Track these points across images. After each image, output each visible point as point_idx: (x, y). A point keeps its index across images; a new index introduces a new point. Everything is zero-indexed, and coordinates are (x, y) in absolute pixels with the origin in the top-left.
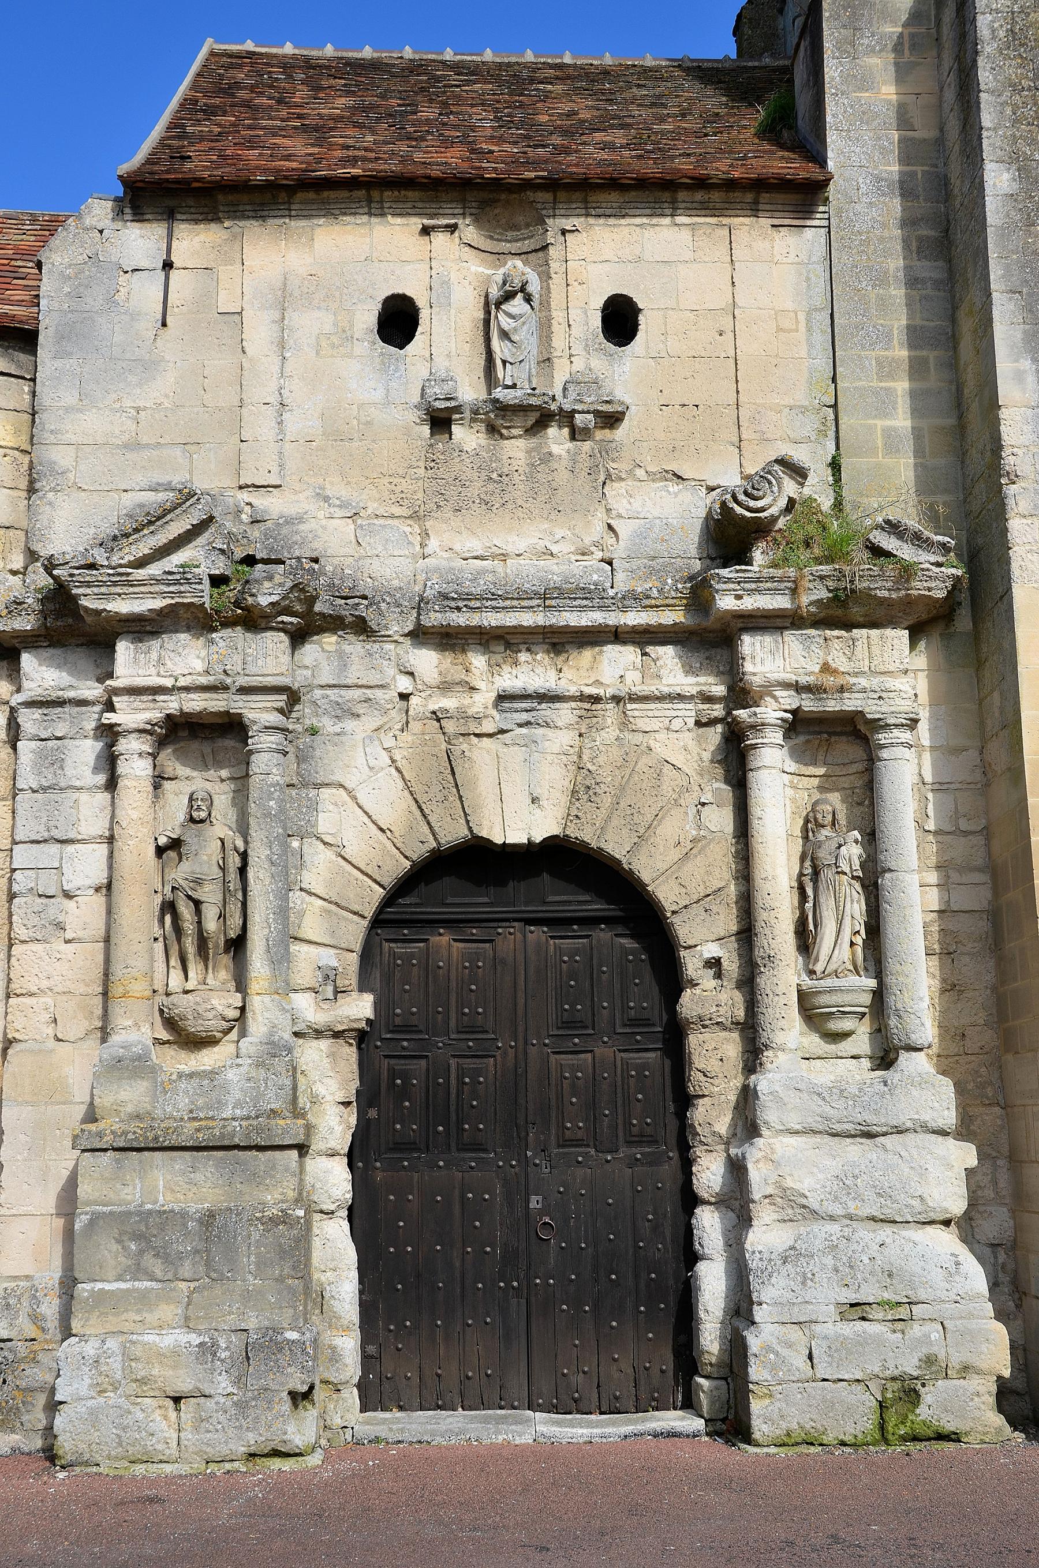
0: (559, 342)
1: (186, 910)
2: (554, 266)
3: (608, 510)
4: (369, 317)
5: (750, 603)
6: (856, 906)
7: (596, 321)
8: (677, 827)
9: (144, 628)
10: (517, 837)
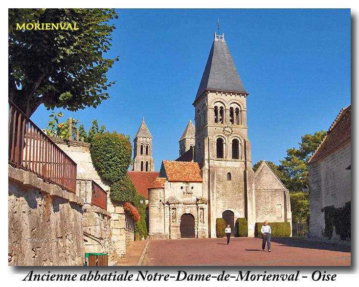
9: (171, 204)
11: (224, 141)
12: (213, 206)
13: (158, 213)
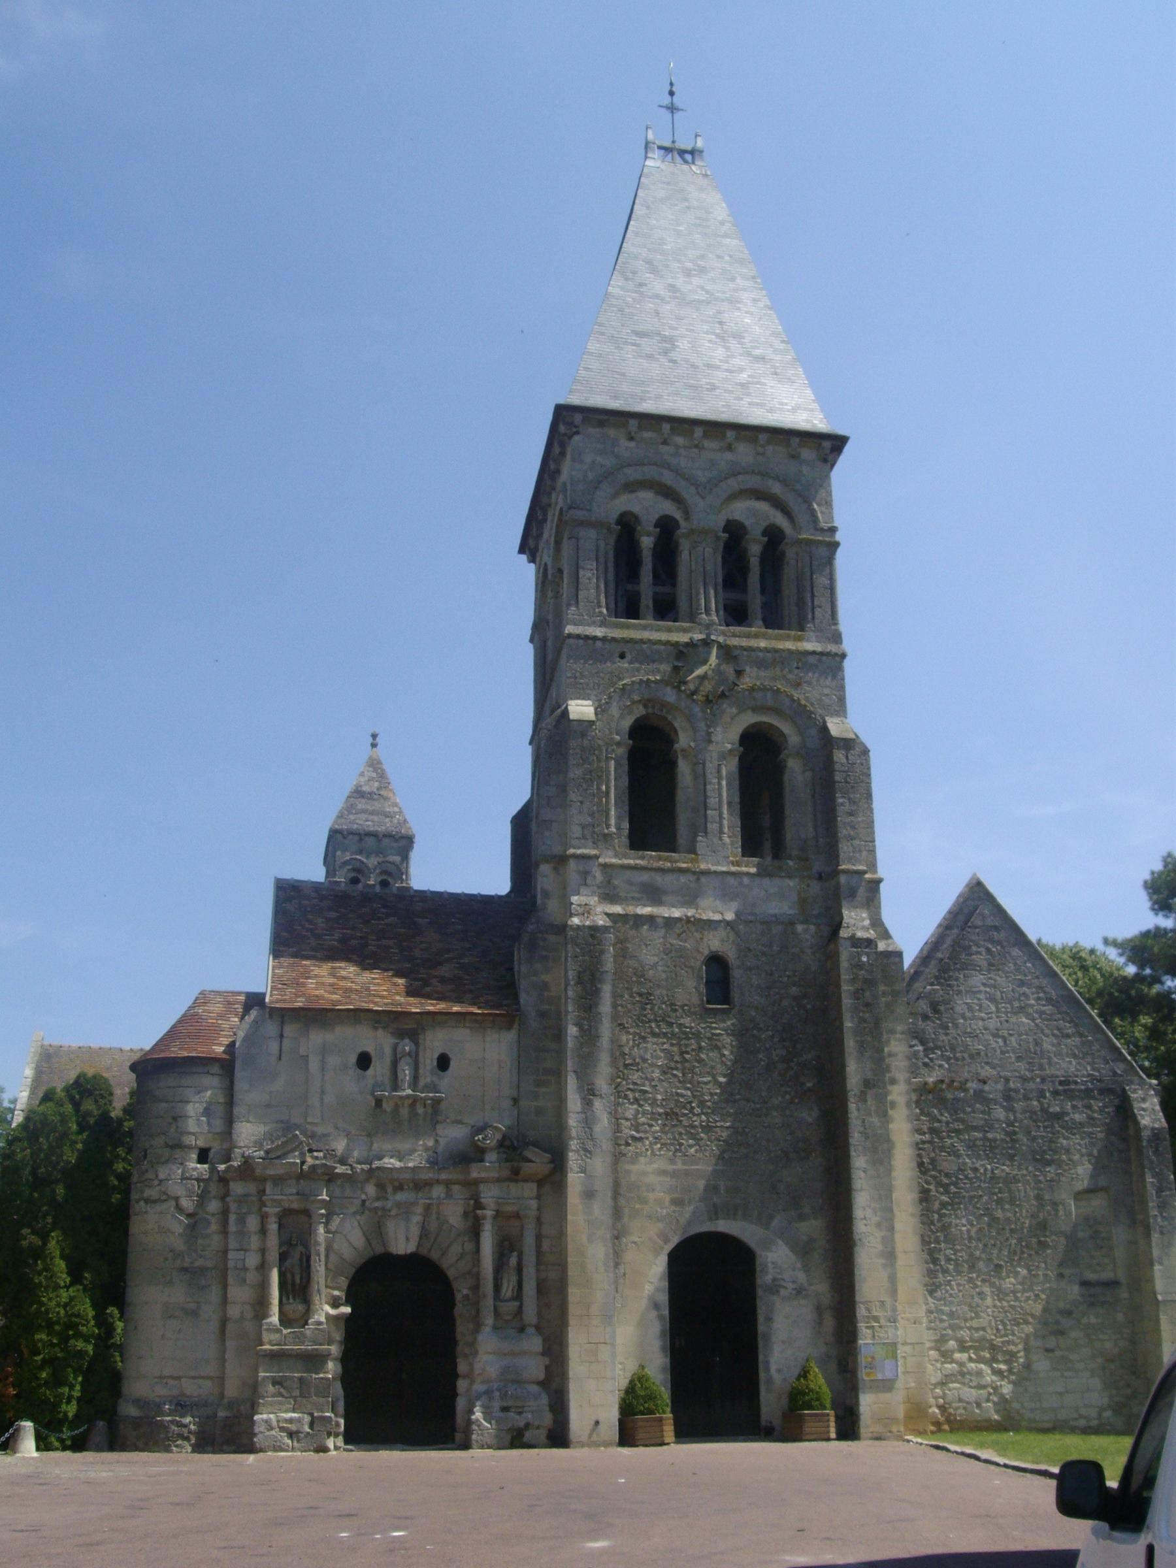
0: (421, 1071)
1: (289, 1276)
4: (353, 1059)
5: (483, 1175)
7: (435, 1063)
8: (456, 1249)
11: (684, 740)
12: (589, 1195)
13: (179, 1245)
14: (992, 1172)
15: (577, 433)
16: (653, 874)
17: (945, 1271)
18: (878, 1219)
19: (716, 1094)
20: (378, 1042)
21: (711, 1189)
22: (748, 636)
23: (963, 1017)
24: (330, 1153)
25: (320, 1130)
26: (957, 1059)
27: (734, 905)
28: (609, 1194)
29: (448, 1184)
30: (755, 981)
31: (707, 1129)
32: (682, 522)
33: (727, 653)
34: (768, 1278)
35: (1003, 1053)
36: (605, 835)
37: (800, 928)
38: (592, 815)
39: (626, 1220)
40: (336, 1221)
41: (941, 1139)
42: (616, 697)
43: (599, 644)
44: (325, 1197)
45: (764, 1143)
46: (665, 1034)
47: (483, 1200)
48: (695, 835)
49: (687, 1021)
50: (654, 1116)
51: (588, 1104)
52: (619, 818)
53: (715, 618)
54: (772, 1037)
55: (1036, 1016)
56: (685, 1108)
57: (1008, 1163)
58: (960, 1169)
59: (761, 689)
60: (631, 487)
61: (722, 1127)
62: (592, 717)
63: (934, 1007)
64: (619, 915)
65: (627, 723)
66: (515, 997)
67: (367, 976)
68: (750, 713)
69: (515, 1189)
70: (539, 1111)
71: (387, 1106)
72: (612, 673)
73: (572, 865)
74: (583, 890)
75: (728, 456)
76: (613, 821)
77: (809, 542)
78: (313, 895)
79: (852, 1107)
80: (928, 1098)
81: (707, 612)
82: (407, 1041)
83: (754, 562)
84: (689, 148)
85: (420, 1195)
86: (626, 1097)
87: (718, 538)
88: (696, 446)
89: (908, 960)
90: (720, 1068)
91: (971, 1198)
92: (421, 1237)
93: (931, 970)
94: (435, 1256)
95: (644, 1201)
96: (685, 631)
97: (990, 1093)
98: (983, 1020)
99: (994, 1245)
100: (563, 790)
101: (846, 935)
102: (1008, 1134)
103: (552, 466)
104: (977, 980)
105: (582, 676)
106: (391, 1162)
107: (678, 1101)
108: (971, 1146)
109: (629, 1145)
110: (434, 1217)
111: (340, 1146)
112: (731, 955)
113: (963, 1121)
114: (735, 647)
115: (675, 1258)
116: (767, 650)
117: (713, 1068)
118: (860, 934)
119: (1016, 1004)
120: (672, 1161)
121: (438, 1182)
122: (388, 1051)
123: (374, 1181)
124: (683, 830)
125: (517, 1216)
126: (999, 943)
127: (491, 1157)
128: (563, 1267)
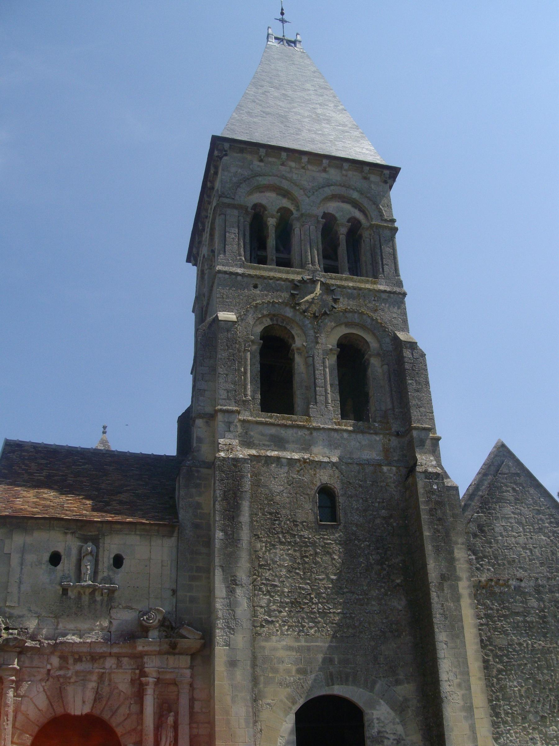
0: (100, 567)
2: (101, 545)
3: (111, 617)
4: (46, 557)
5: (146, 648)
6: (172, 734)
8: (124, 710)
10: (78, 712)
11: (299, 342)
12: (232, 664)
14: (533, 646)
15: (226, 155)
16: (279, 428)
17: (505, 723)
18: (458, 680)
19: (329, 588)
20: (66, 544)
21: (328, 661)
22: (341, 279)
23: (502, 535)
24: (23, 631)
25: (16, 612)
26: (499, 565)
27: (338, 452)
28: (249, 663)
29: (118, 657)
30: (355, 505)
31: (324, 614)
32: (294, 212)
33: (326, 288)
34: (374, 731)
35: (530, 560)
36: (244, 401)
37: (385, 469)
38: (235, 383)
39: (261, 686)
40: (25, 686)
41: (494, 622)
42: (251, 311)
43: (239, 278)
44: (16, 666)
45: (366, 625)
46: (289, 543)
47: (146, 670)
48: (308, 404)
49: (306, 533)
50: (282, 605)
51: (231, 591)
52: (253, 392)
53: (317, 267)
54: (369, 546)
55: (550, 534)
56: (305, 598)
57: (542, 639)
58: (509, 644)
59: (351, 312)
60: (262, 189)
61: (334, 613)
62: (236, 320)
63: (481, 528)
64: (254, 456)
65: (259, 329)
66: (175, 514)
67: (64, 498)
68: (343, 327)
69: (172, 661)
70: (193, 600)
71: (72, 594)
72: (248, 296)
73: (220, 417)
74: (227, 434)
75: (324, 175)
76: (249, 393)
77: (378, 227)
78: (32, 450)
79: (434, 595)
80: (483, 592)
81: (313, 263)
82: (90, 544)
83: (342, 238)
84: (293, 40)
85: (96, 665)
86: (260, 589)
87: (318, 222)
88: (303, 168)
89: (462, 492)
90: (331, 569)
91: (519, 665)
92: (95, 700)
93: (476, 503)
94: (106, 716)
95: (275, 670)
96: (298, 273)
97: (525, 588)
98: (515, 537)
99: (539, 701)
100: (213, 369)
101: (421, 470)
102: (540, 617)
103: (209, 184)
104: (508, 510)
105: (228, 297)
106: (73, 638)
107: (300, 593)
108: (516, 626)
109: (263, 626)
110: (106, 683)
111: (32, 624)
112: (337, 486)
113: (508, 609)
114: (333, 285)
115: (300, 716)
116: (354, 288)
117: (325, 568)
118: (430, 470)
119: (536, 526)
120: (297, 639)
121: (110, 654)
122: (74, 552)
123: (58, 654)
124: (299, 401)
125: (174, 683)
126: (521, 484)
127: (154, 634)
128: (211, 723)
